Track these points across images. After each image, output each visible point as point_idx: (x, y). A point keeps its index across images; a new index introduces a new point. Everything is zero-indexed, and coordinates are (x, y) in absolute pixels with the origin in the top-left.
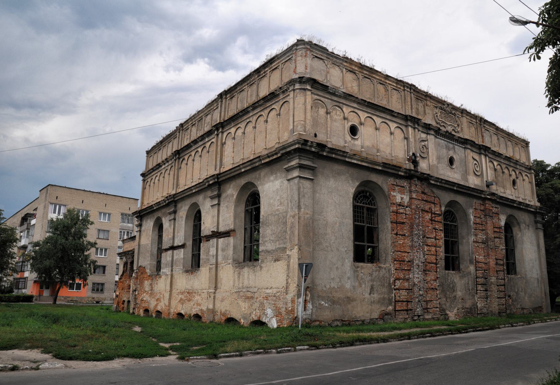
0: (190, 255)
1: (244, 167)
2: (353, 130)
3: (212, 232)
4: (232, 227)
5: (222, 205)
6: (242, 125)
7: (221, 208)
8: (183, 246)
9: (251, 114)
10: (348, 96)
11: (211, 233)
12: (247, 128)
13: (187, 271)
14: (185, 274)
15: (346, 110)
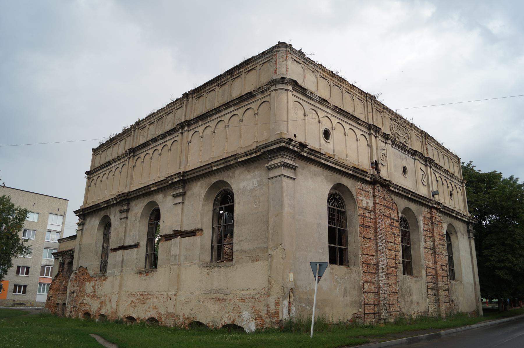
0: (144, 255)
1: (216, 166)
2: (327, 134)
3: (174, 231)
4: (199, 226)
5: (186, 202)
6: (213, 124)
7: (185, 207)
8: (136, 246)
9: (223, 113)
10: (323, 101)
11: (172, 233)
12: (217, 127)
13: (141, 273)
14: (138, 276)
15: (321, 114)
